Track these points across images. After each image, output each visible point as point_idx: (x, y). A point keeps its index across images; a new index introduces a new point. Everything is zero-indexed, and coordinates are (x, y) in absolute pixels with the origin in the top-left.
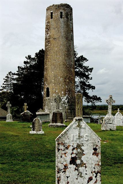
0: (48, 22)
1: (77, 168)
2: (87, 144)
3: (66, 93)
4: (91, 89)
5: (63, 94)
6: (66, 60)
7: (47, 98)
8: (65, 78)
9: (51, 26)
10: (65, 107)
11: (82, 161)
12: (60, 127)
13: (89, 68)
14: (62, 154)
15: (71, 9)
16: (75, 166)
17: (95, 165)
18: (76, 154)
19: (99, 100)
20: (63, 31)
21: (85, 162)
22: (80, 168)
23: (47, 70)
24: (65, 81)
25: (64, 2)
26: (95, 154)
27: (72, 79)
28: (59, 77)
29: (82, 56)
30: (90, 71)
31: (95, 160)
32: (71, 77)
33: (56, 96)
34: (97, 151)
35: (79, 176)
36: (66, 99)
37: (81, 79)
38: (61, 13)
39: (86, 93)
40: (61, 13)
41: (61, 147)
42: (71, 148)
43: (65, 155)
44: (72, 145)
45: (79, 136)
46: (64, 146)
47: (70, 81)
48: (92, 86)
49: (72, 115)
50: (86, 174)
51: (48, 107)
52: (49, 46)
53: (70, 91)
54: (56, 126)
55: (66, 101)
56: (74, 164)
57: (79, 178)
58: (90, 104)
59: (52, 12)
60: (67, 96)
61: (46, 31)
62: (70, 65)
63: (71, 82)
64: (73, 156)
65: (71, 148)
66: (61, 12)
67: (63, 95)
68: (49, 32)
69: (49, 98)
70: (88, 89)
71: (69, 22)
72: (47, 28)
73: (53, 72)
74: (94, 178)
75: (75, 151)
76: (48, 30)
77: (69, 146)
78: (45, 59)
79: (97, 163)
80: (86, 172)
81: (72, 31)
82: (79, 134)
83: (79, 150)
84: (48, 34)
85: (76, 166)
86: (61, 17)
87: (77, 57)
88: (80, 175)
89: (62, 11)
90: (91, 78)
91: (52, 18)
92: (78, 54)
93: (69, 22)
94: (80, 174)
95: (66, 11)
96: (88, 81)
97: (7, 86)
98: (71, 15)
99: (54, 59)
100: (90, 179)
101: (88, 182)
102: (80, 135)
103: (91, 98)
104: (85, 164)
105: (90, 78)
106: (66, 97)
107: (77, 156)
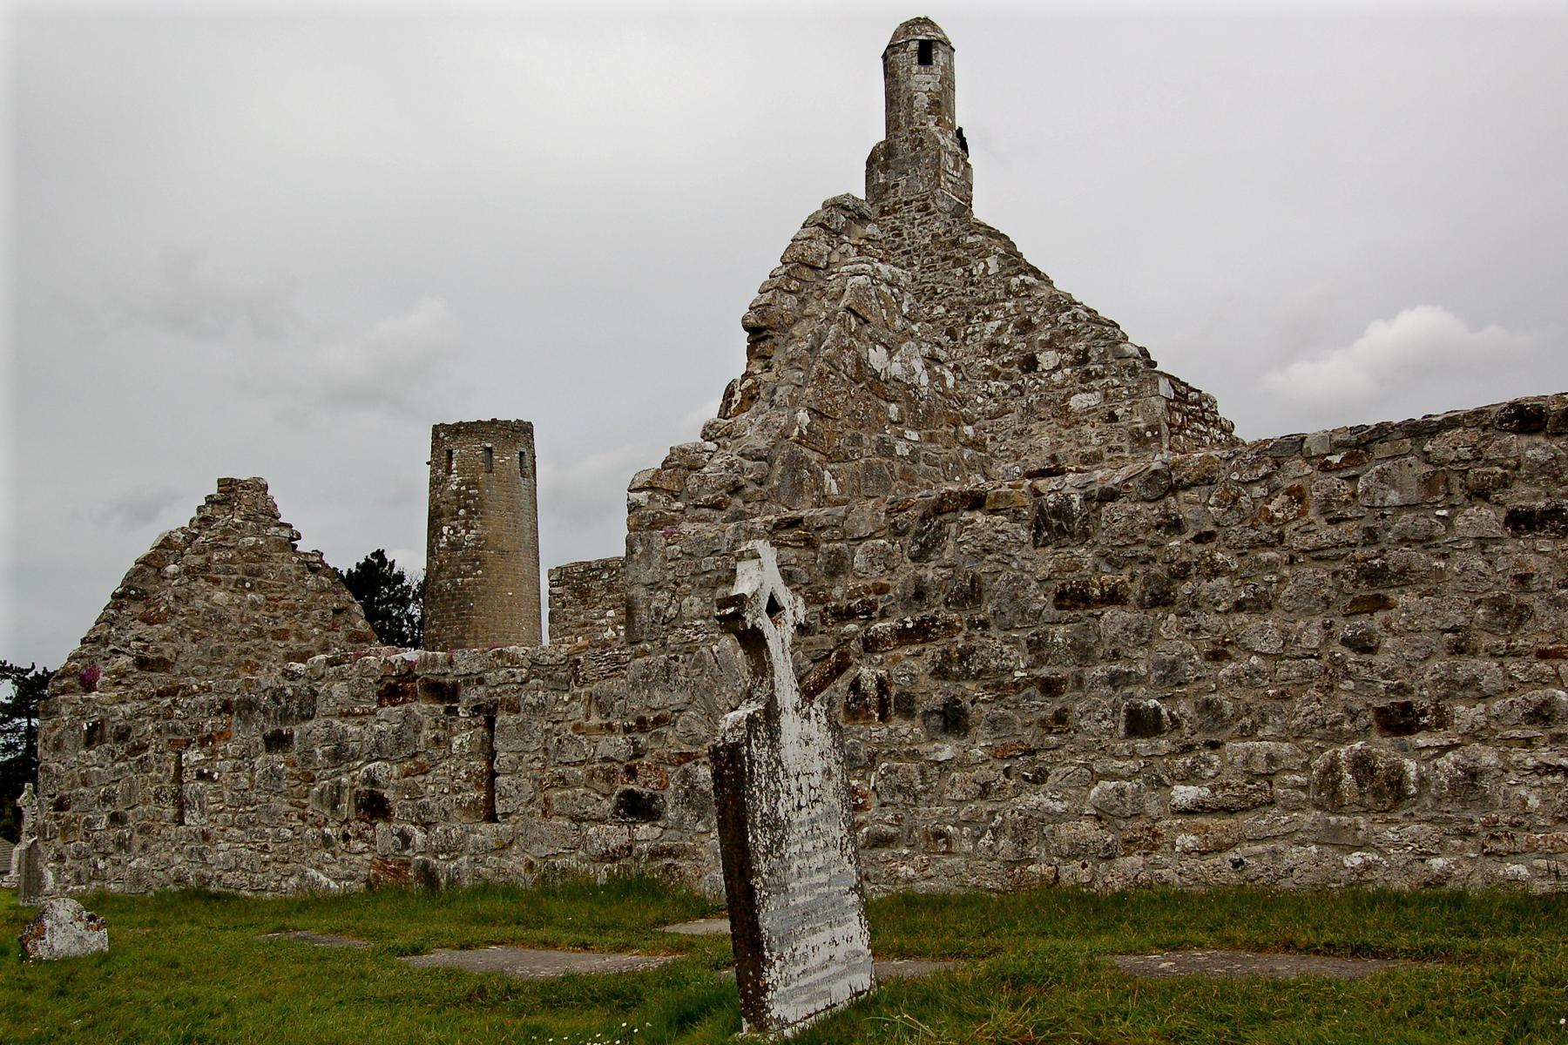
40: (522, 454)
52: (475, 577)
59: (489, 445)
72: (466, 507)
76: (469, 512)
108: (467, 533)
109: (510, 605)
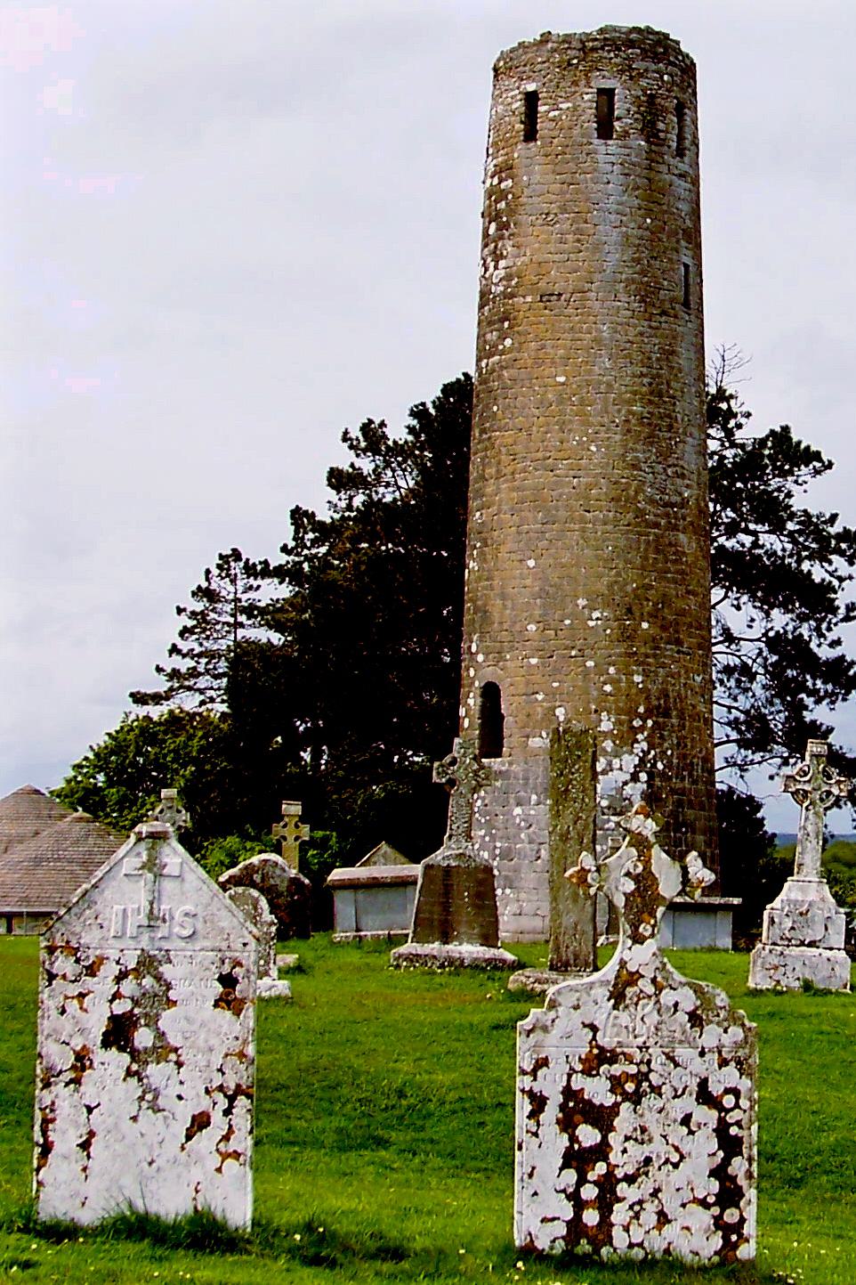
0: (504, 170)
1: (135, 1067)
2: (189, 953)
3: (635, 731)
5: (605, 735)
6: (634, 467)
8: (629, 611)
9: (523, 200)
11: (161, 1035)
12: (476, 966)
13: (835, 529)
14: (67, 997)
15: (688, 70)
16: (126, 1058)
17: (227, 1055)
18: (136, 1003)
20: (615, 236)
21: (174, 1040)
22: (152, 1069)
24: (627, 636)
25: (627, 18)
26: (228, 1003)
27: (682, 613)
28: (582, 602)
29: (786, 429)
30: (842, 553)
31: (224, 1030)
32: (681, 604)
34: (238, 987)
35: (145, 1105)
36: (635, 778)
37: (768, 614)
38: (606, 95)
40: (606, 95)
41: (64, 965)
42: (109, 970)
43: (81, 1003)
44: (113, 954)
45: (151, 915)
46: (78, 961)
47: (664, 628)
50: (180, 1097)
52: (502, 353)
53: (667, 714)
54: (442, 966)
55: (635, 791)
56: (122, 1049)
57: (147, 1116)
59: (531, 87)
60: (638, 748)
61: (486, 234)
62: (672, 505)
63: (679, 642)
64: (121, 1007)
65: (109, 970)
66: (601, 92)
68: (508, 247)
71: (664, 168)
73: (531, 563)
74: (217, 1116)
75: (128, 986)
76: (503, 227)
77: (101, 960)
78: (476, 459)
79: (237, 1048)
80: (179, 1090)
82: (151, 903)
83: (148, 982)
84: (502, 257)
85: (133, 1060)
86: (605, 130)
87: (739, 435)
88: (151, 1100)
91: (530, 135)
92: (748, 415)
93: (664, 168)
94: (149, 1097)
95: (643, 83)
96: (831, 636)
97: (201, 669)
98: (680, 110)
99: (540, 455)
100: (200, 1122)
101: (189, 1137)
102: (155, 912)
104: (176, 1050)
105: (842, 611)
106: (630, 762)
107: (136, 1011)
108: (496, 268)
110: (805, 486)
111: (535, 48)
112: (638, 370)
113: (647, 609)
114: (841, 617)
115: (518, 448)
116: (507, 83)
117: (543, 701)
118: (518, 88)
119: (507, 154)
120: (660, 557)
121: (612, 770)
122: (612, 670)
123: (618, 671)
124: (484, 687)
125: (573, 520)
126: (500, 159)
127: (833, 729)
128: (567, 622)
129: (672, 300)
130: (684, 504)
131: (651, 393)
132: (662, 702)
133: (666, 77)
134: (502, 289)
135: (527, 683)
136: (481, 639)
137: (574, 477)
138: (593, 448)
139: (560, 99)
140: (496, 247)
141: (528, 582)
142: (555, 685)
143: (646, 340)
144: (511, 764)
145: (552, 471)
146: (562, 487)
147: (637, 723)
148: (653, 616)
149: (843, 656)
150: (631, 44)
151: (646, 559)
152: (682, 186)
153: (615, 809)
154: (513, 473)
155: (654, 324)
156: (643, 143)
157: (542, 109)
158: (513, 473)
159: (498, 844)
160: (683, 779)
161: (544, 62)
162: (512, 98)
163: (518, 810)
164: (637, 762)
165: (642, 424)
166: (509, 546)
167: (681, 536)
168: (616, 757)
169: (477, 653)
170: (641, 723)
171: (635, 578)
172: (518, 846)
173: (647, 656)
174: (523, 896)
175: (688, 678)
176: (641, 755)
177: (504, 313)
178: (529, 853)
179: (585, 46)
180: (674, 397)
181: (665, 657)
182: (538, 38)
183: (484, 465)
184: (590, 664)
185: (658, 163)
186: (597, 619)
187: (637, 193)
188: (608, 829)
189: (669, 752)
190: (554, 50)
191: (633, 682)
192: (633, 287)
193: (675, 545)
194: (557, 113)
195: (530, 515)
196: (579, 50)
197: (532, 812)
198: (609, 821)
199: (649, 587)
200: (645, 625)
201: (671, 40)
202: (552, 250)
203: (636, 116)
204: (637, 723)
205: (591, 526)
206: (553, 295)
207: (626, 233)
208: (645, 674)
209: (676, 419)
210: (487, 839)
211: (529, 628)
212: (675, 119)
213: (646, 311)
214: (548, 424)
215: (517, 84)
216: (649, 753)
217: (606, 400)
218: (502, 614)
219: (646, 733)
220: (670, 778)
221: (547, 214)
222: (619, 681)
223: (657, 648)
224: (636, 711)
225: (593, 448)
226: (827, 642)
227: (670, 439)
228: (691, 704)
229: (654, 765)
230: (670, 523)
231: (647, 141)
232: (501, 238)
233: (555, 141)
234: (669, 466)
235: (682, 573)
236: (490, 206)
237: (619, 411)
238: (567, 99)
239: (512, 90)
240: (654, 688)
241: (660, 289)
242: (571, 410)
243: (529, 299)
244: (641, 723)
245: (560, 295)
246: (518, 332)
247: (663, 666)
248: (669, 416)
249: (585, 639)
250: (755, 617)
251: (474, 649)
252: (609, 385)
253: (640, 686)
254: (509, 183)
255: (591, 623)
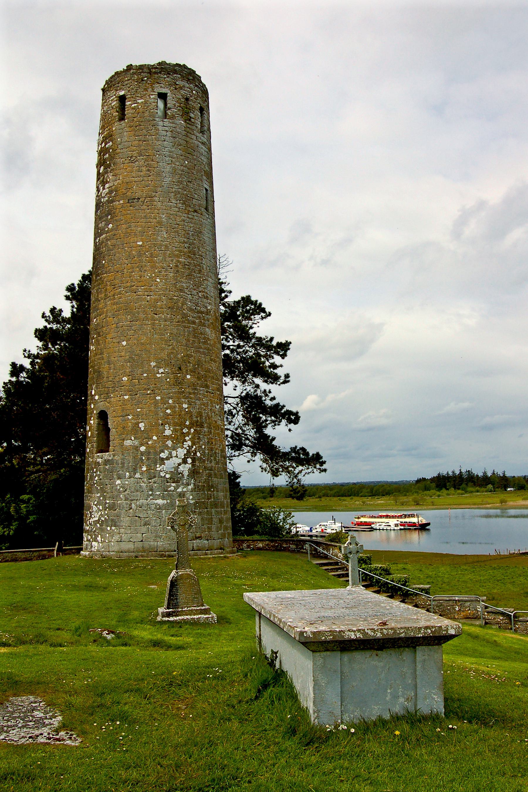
3: (184, 435)
4: (284, 422)
5: (168, 438)
6: (181, 290)
7: (100, 458)
9: (118, 151)
10: (182, 495)
13: (274, 343)
19: (318, 466)
20: (168, 169)
23: (99, 335)
24: (178, 382)
27: (208, 371)
28: (153, 364)
30: (278, 353)
32: (207, 366)
33: (137, 448)
36: (185, 461)
39: (267, 437)
47: (199, 379)
48: (289, 413)
49: (210, 529)
51: (105, 498)
52: (107, 232)
53: (202, 426)
55: (185, 469)
58: (282, 480)
59: (122, 93)
61: (99, 173)
62: (202, 313)
63: (207, 386)
67: (169, 443)
69: (106, 455)
70: (273, 421)
73: (124, 343)
81: (209, 175)
84: (107, 182)
89: (164, 91)
90: (287, 376)
91: (122, 118)
92: (230, 292)
95: (182, 92)
98: (201, 110)
99: (128, 284)
103: (285, 456)
105: (282, 379)
106: (182, 452)
108: (104, 189)
109: (140, 255)
110: (258, 324)
111: (124, 73)
112: (182, 239)
113: (189, 368)
114: (281, 381)
115: (117, 281)
116: (109, 94)
117: (132, 419)
118: (115, 95)
119: (109, 129)
120: (196, 340)
121: (172, 457)
122: (171, 401)
123: (174, 401)
124: (99, 413)
125: (147, 319)
126: (106, 133)
127: (275, 438)
128: (145, 375)
129: (200, 205)
130: (208, 312)
131: (190, 252)
132: (199, 419)
133: (194, 92)
134: (107, 199)
135: (123, 411)
136: (97, 388)
137: (148, 296)
138: (158, 280)
139: (138, 98)
140: (104, 178)
141: (123, 354)
142: (138, 410)
143: (186, 224)
144: (114, 456)
145: (135, 293)
146: (141, 301)
147: (185, 431)
148: (193, 372)
149: (279, 403)
150: (175, 72)
151: (188, 340)
152: (203, 149)
153: (174, 479)
154: (114, 295)
155: (190, 216)
156: (183, 122)
157: (128, 103)
158: (114, 295)
159: (108, 502)
160: (211, 462)
161: (129, 80)
162: (112, 101)
163: (118, 482)
164: (185, 453)
165: (185, 268)
166: (113, 335)
167: (207, 329)
168: (174, 449)
169: (95, 395)
170: (187, 430)
171: (183, 350)
172: (119, 502)
173: (190, 393)
174: (122, 531)
175: (213, 406)
176: (188, 448)
177: (108, 211)
178: (125, 506)
179: (151, 71)
180: (202, 256)
181: (200, 394)
182: (125, 68)
183: (98, 294)
184: (158, 398)
185: (190, 133)
186: (162, 373)
187: (180, 147)
188: (170, 491)
189: (203, 447)
190: (134, 74)
191: (183, 408)
192: (179, 196)
193: (204, 334)
194: (136, 105)
195: (124, 317)
196: (148, 73)
197: (127, 482)
198: (171, 486)
199: (190, 356)
200: (188, 377)
201: (197, 74)
202: (134, 175)
203: (178, 108)
204: (185, 431)
205: (157, 322)
206: (134, 199)
207: (174, 167)
208: (189, 403)
209: (203, 268)
210: (101, 498)
211: (123, 379)
212: (200, 114)
213: (186, 209)
214: (133, 268)
215: (114, 93)
216: (193, 447)
217: (165, 254)
218: (108, 372)
219: (190, 436)
220: (204, 461)
221: (131, 157)
222: (175, 407)
223: (196, 389)
224: (185, 424)
225: (158, 280)
226: (269, 398)
227: (200, 277)
228: (214, 421)
229: (195, 454)
230: (201, 322)
231: (185, 122)
232: (106, 172)
233: (135, 119)
234: (200, 292)
235: (208, 349)
236: (101, 158)
237: (172, 261)
238: (141, 98)
239: (112, 97)
240: (194, 411)
241: (193, 198)
242: (146, 260)
243: (121, 202)
244: (187, 430)
245: (139, 199)
246: (116, 220)
247: (199, 399)
248: (199, 265)
249: (155, 384)
250: (237, 385)
251: (93, 393)
252: (166, 246)
253: (187, 410)
254: (111, 143)
255: (158, 375)
